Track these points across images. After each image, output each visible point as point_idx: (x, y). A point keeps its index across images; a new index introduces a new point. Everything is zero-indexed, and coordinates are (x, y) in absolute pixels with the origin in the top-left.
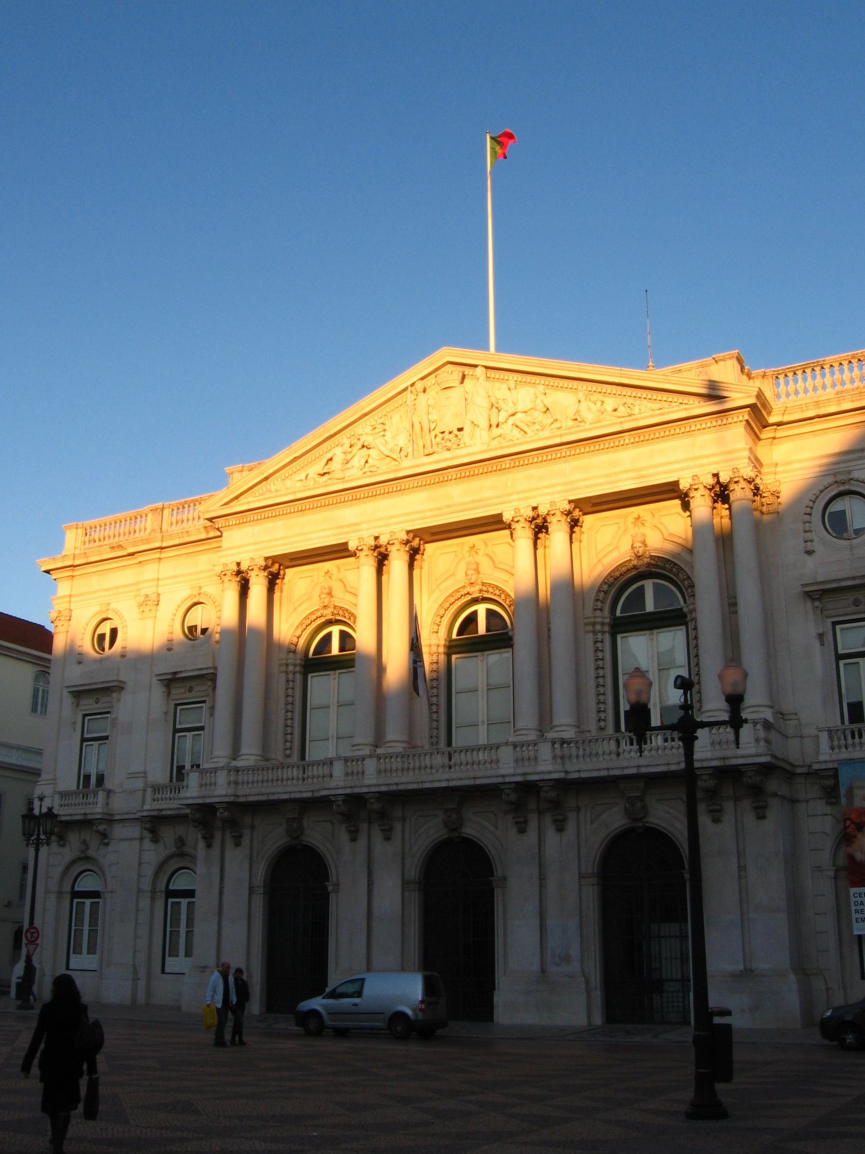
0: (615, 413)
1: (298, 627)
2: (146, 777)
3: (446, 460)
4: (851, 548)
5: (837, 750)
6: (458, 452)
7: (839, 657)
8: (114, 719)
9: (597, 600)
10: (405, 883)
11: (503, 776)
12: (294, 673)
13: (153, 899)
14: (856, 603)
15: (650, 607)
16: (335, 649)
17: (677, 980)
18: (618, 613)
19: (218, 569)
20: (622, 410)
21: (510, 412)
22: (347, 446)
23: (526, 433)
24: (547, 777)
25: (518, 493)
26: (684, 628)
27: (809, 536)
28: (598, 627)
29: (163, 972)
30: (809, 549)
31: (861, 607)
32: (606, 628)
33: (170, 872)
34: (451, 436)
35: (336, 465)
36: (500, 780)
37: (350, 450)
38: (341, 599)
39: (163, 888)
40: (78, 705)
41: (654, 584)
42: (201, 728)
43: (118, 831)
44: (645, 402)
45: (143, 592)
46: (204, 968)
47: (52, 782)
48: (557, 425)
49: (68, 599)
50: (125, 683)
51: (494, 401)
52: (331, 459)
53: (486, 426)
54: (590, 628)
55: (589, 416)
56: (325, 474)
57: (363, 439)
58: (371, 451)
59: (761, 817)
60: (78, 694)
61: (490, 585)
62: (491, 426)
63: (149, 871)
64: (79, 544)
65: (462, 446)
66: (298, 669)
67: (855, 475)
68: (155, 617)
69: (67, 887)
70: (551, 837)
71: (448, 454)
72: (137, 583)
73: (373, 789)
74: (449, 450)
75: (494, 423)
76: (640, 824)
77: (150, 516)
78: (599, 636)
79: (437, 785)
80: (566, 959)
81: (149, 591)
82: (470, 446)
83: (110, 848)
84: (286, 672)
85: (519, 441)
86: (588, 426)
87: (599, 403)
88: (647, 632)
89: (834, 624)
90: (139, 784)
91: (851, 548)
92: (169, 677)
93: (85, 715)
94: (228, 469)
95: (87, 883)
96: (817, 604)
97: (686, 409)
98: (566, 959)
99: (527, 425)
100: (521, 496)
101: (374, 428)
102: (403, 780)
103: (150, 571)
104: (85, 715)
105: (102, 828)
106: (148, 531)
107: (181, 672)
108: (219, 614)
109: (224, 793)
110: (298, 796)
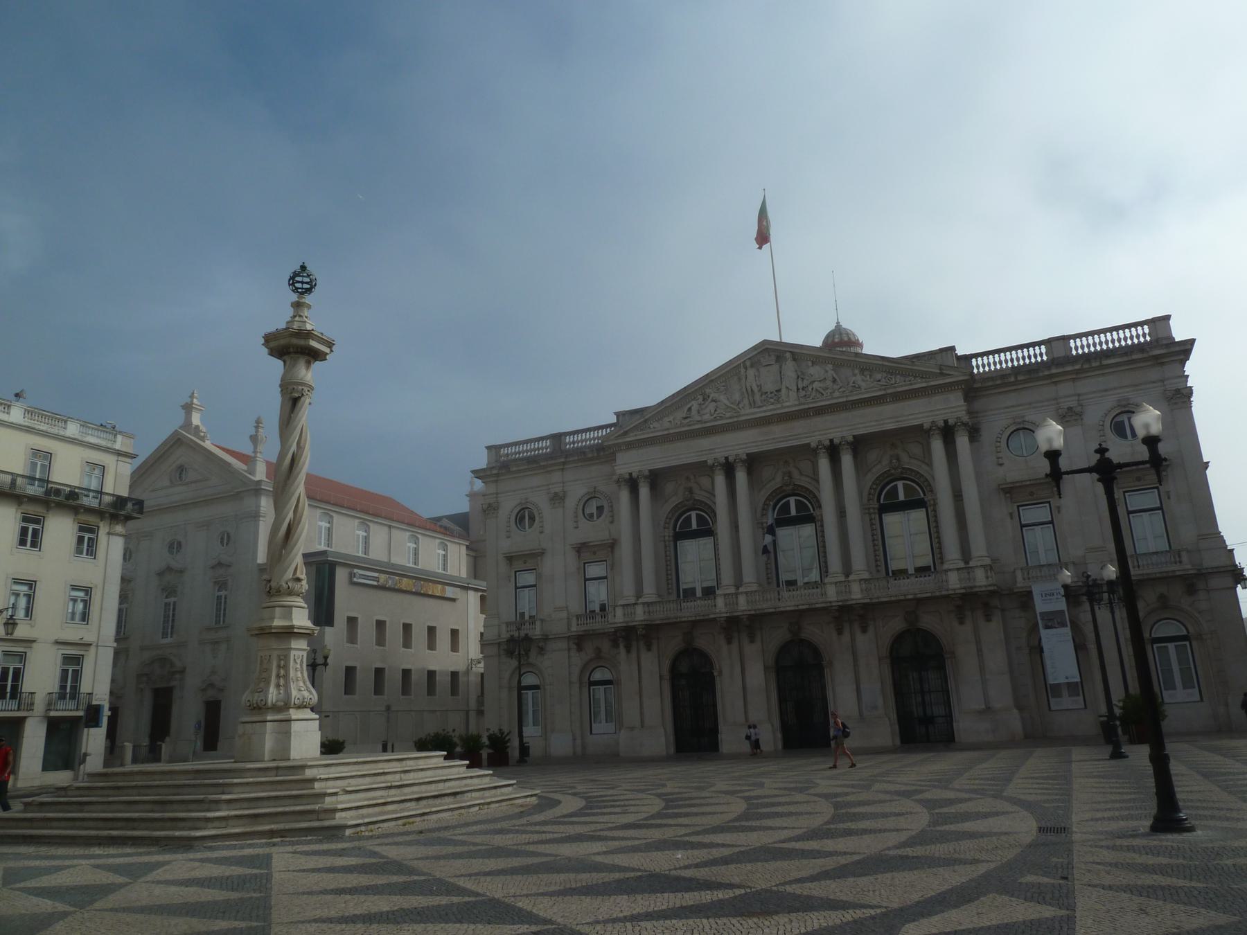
0: (879, 383)
1: (669, 513)
2: (567, 610)
3: (771, 410)
5: (1027, 581)
6: (779, 406)
9: (870, 494)
10: (766, 668)
11: (830, 602)
12: (669, 541)
13: (580, 688)
14: (1032, 494)
15: (902, 497)
16: (694, 526)
17: (943, 717)
18: (882, 502)
19: (615, 477)
23: (823, 395)
24: (859, 602)
25: (820, 431)
26: (924, 510)
27: (1000, 455)
28: (872, 510)
29: (591, 733)
30: (1000, 462)
31: (1035, 496)
32: (876, 511)
33: (591, 669)
34: (773, 395)
35: (694, 412)
36: (829, 605)
37: (702, 402)
38: (700, 495)
40: (511, 565)
41: (903, 484)
46: (632, 729)
49: (495, 495)
50: (545, 550)
51: (799, 374)
52: (690, 409)
53: (796, 390)
54: (867, 511)
55: (863, 384)
57: (712, 396)
59: (989, 620)
60: (510, 559)
61: (800, 486)
62: (798, 389)
66: (671, 538)
67: (1027, 419)
68: (564, 507)
70: (860, 638)
71: (772, 407)
72: (548, 485)
73: (745, 613)
74: (772, 404)
75: (800, 386)
78: (873, 516)
79: (788, 609)
81: (557, 490)
82: (786, 402)
86: (863, 391)
87: (868, 376)
88: (901, 512)
89: (1018, 506)
90: (564, 614)
92: (579, 546)
95: (529, 680)
96: (1008, 495)
99: (824, 390)
102: (764, 606)
103: (556, 477)
105: (540, 644)
108: (610, 504)
109: (642, 618)
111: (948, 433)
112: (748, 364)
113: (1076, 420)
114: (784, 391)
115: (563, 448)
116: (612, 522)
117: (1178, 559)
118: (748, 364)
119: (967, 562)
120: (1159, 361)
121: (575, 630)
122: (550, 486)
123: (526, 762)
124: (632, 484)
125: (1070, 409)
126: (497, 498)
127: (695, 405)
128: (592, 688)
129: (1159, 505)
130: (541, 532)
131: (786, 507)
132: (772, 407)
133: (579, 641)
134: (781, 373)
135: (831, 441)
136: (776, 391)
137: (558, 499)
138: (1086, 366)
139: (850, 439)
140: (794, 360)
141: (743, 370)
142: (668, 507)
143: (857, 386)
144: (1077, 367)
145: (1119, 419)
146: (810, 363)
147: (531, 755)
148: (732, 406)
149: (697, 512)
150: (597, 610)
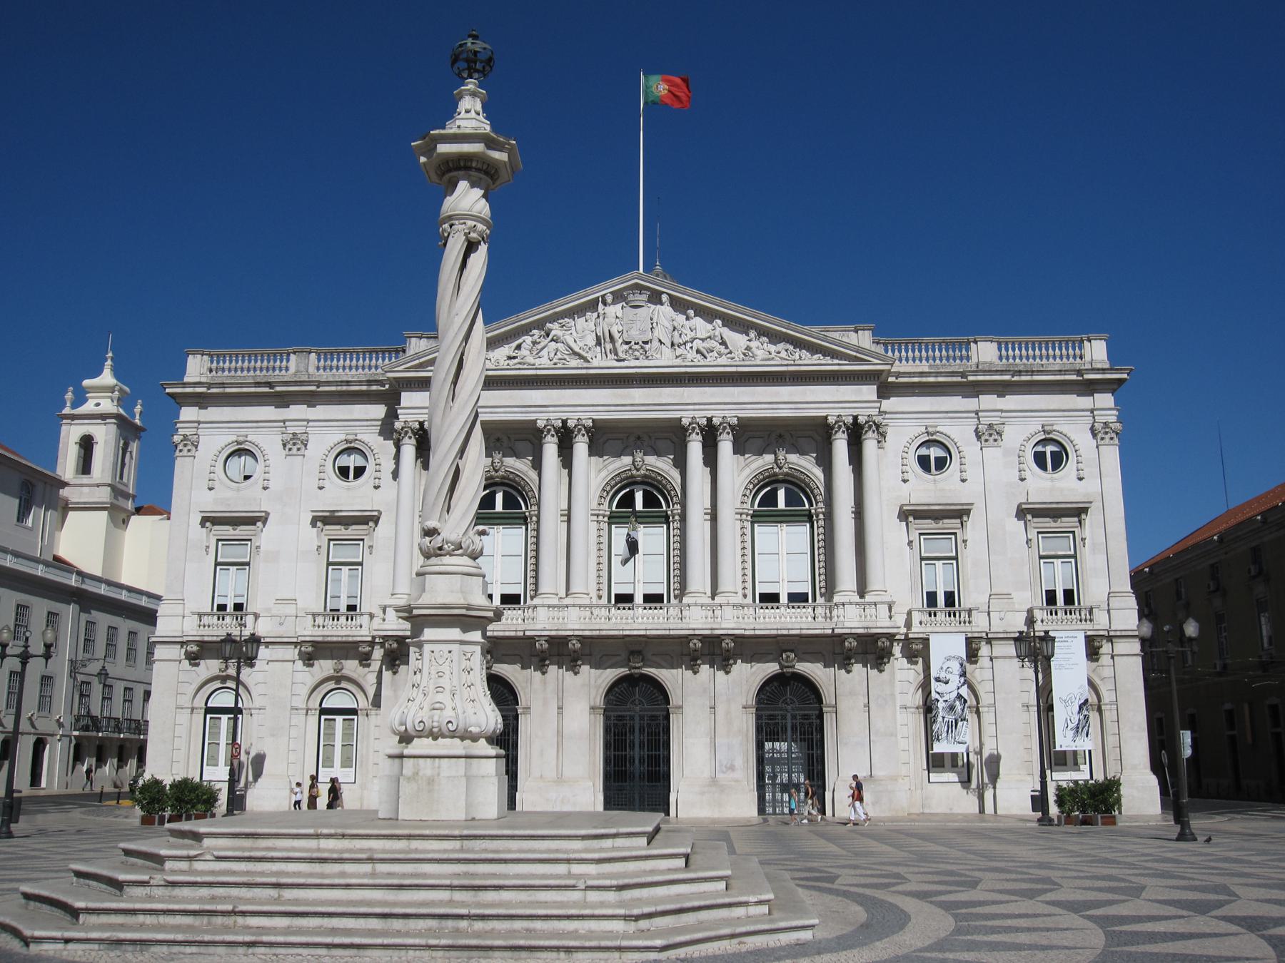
4: (935, 482)
7: (922, 559)
8: (258, 547)
10: (592, 708)
20: (783, 354)
21: (689, 337)
22: (536, 337)
31: (940, 524)
34: (637, 347)
35: (524, 352)
36: (691, 632)
39: (317, 706)
42: (361, 564)
43: (263, 652)
45: (291, 430)
47: (181, 602)
48: (729, 355)
52: (519, 347)
53: (670, 346)
55: (760, 354)
56: (515, 358)
57: (553, 333)
58: (560, 345)
60: (210, 520)
62: (673, 345)
63: (305, 691)
64: (205, 370)
65: (650, 358)
69: (199, 701)
72: (284, 421)
74: (638, 359)
76: (790, 670)
77: (293, 357)
80: (732, 768)
82: (657, 359)
83: (256, 668)
85: (699, 364)
86: (759, 363)
89: (920, 534)
91: (935, 482)
92: (328, 514)
93: (218, 540)
94: (406, 334)
97: (839, 365)
98: (732, 768)
100: (697, 407)
101: (562, 326)
104: (218, 540)
106: (292, 370)
107: (341, 511)
110: (501, 634)
111: (856, 433)
112: (609, 299)
113: (995, 440)
114: (656, 344)
115: (312, 370)
116: (376, 487)
117: (1088, 617)
118: (609, 299)
119: (862, 596)
120: (1091, 388)
121: (310, 633)
122: (287, 423)
125: (990, 426)
126: (198, 428)
127: (528, 339)
128: (323, 717)
129: (1072, 552)
130: (265, 488)
131: (628, 501)
132: (637, 363)
133: (313, 651)
134: (651, 319)
135: (709, 420)
136: (643, 342)
137: (296, 443)
138: (1016, 378)
143: (751, 354)
144: (1007, 378)
145: (1040, 448)
146: (691, 312)
147: (247, 809)
148: (581, 352)
149: (506, 489)
150: (343, 609)
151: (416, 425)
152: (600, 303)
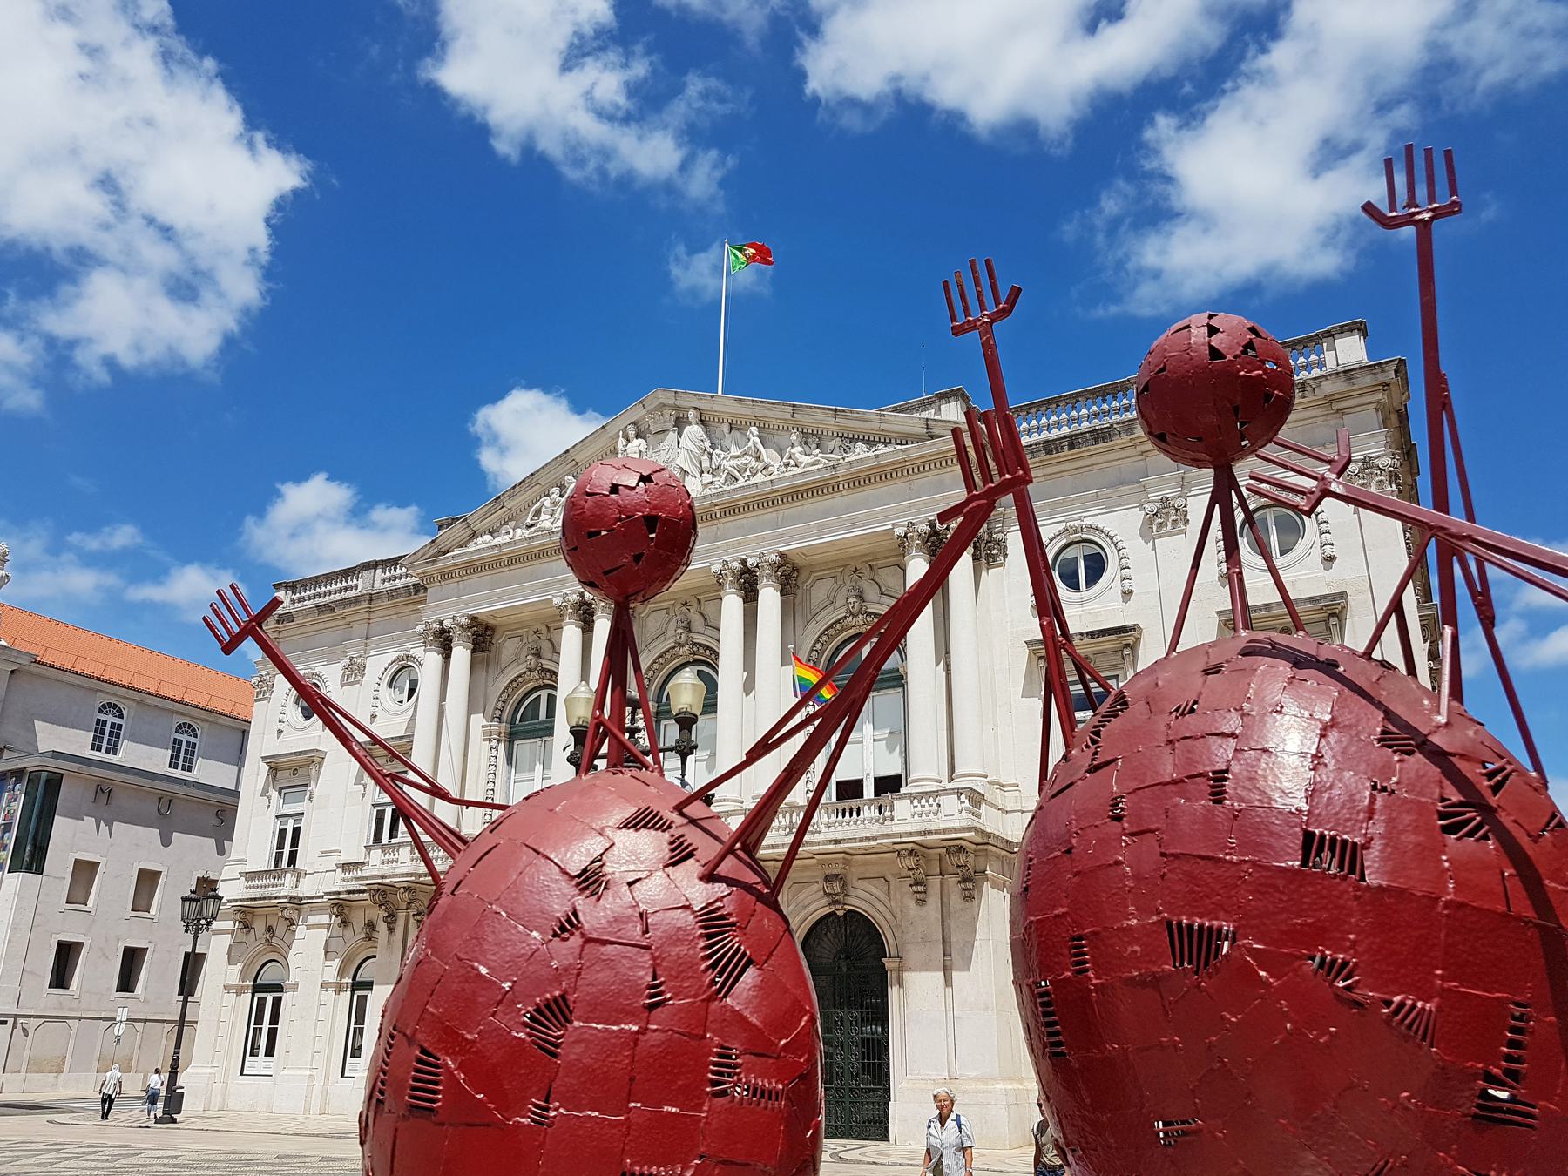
1: (503, 692)
12: (499, 741)
23: (737, 480)
35: (543, 517)
44: (860, 444)
52: (538, 513)
61: (701, 645)
84: (490, 740)
87: (814, 446)
105: (286, 914)
112: (632, 431)
123: (174, 1121)
124: (444, 642)
127: (547, 501)
139: (774, 557)
140: (702, 422)
141: (622, 441)
142: (503, 682)
146: (725, 428)
151: (436, 626)
152: (621, 438)
